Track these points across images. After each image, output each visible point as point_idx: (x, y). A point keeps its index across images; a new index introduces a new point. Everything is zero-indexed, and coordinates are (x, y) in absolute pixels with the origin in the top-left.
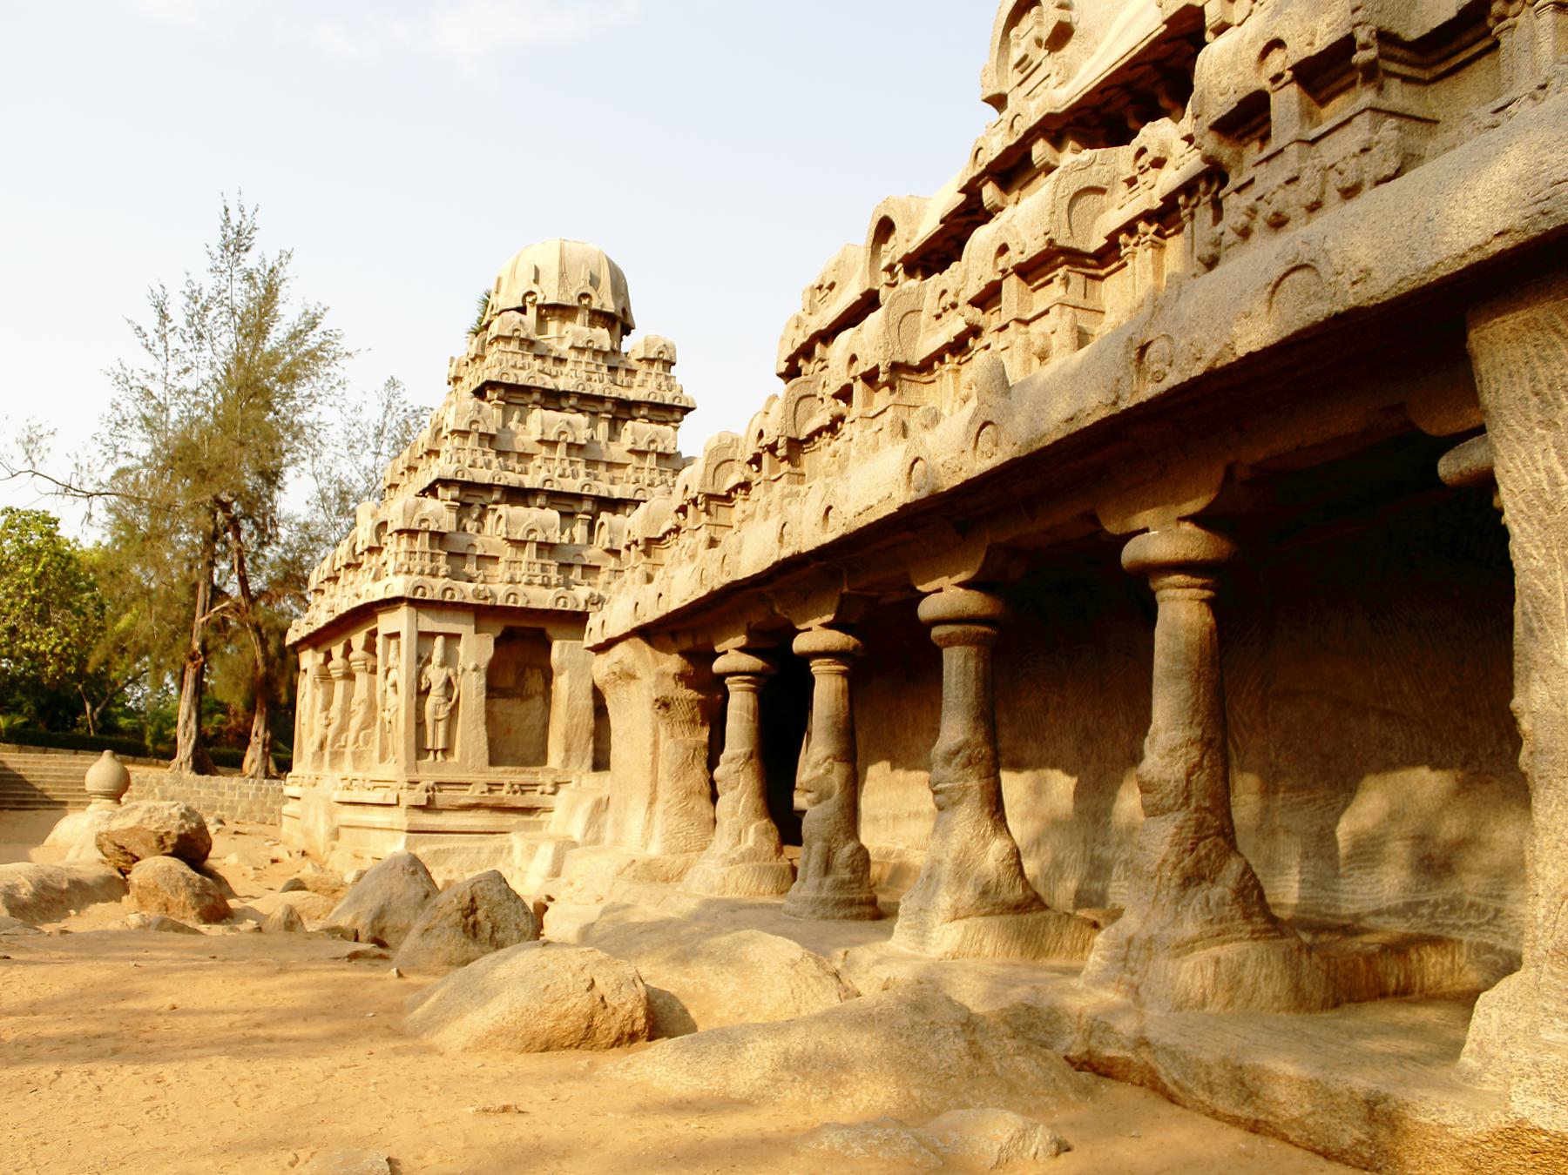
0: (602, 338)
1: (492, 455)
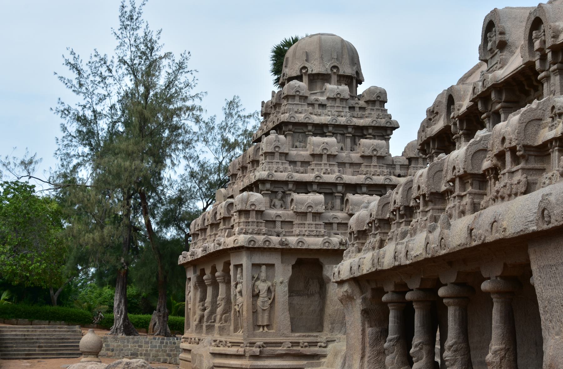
0: (344, 88)
1: (287, 165)
